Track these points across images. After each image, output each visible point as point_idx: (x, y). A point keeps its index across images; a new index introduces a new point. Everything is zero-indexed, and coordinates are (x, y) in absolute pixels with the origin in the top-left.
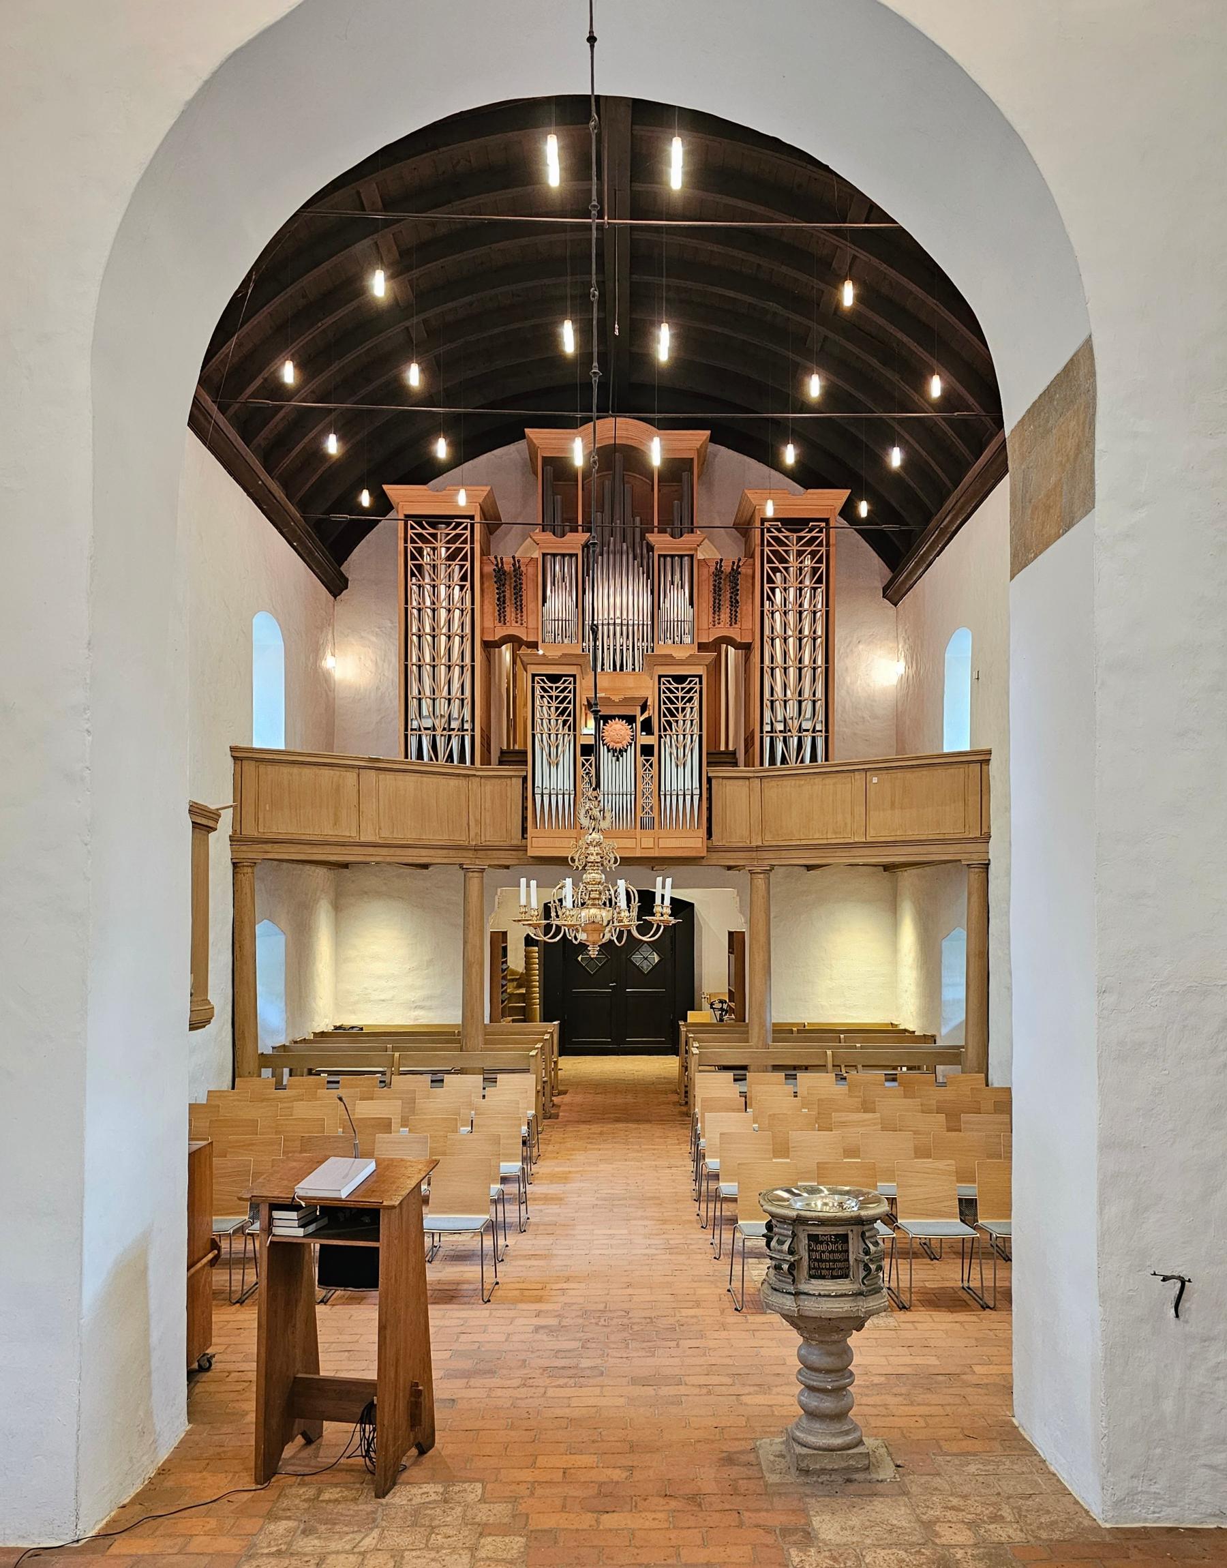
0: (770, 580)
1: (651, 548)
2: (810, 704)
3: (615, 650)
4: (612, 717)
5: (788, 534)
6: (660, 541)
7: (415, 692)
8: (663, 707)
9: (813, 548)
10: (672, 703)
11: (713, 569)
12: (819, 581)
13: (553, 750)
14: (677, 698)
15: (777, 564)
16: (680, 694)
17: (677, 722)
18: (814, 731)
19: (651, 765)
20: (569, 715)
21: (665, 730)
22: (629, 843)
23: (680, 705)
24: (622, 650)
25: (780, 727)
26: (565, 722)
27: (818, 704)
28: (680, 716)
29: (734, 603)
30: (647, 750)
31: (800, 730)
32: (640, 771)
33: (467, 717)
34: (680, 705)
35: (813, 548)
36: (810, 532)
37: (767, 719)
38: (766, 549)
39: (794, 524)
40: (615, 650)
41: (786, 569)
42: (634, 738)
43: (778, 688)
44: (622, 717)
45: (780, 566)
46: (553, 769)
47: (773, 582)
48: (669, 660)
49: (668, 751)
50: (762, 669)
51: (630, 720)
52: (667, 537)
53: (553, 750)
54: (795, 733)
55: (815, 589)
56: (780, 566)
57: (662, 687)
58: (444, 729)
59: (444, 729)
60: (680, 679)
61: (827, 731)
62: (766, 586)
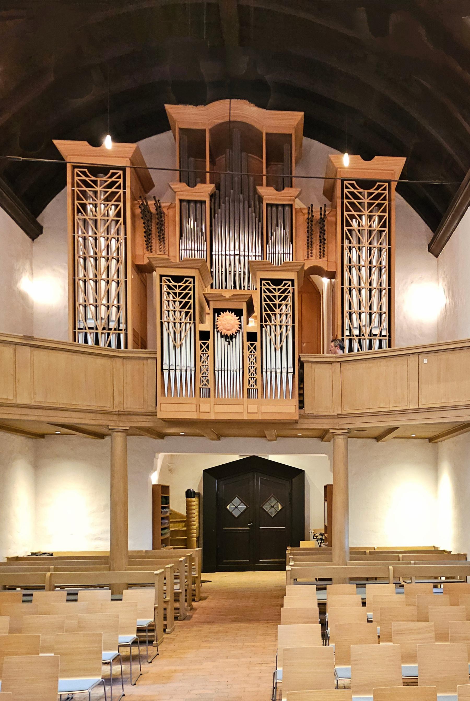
4: (224, 310)
10: (271, 300)
14: (275, 297)
20: (190, 308)
23: (277, 302)
26: (187, 313)
28: (277, 311)
34: (277, 302)
51: (239, 313)
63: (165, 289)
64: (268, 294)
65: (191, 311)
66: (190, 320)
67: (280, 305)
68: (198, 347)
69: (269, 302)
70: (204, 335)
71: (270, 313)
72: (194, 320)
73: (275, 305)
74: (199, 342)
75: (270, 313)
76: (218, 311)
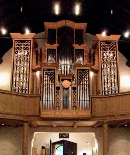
0: (103, 55)
1: (73, 48)
2: (114, 84)
3: (65, 71)
4: (66, 80)
5: (106, 45)
6: (76, 47)
7: (14, 80)
8: (78, 77)
9: (112, 48)
10: (81, 76)
11: (88, 53)
12: (114, 55)
13: (48, 88)
14: (82, 75)
15: (104, 51)
16: (83, 74)
17: (82, 81)
18: (115, 90)
19: (76, 92)
21: (79, 83)
22: (70, 114)
23: (83, 77)
24: (66, 71)
25: (107, 89)
27: (116, 84)
28: (83, 80)
29: (94, 60)
30: (74, 89)
31: (112, 90)
32: (73, 94)
33: (27, 86)
34: (83, 77)
35: (112, 48)
36: (112, 44)
37: (103, 87)
38: (101, 48)
39: (108, 43)
40: (65, 71)
41: (107, 52)
42: (71, 85)
43: (106, 79)
44: (68, 80)
45: (105, 52)
46: (48, 93)
47: (103, 55)
48: (80, 65)
49: (80, 88)
50: (102, 75)
51: (70, 80)
52: (77, 45)
53: (48, 88)
54: (110, 90)
55: (113, 57)
56: (105, 52)
57: (78, 72)
58: (21, 89)
59: (21, 89)
60: (83, 70)
61: (118, 90)
62: (102, 56)
63: (45, 73)
64: (80, 74)
65: (54, 80)
66: (53, 83)
67: (84, 78)
68: (55, 92)
69: (80, 77)
70: (58, 88)
71: (81, 80)
72: (54, 83)
73: (82, 78)
74: (56, 91)
75: (81, 80)
76: (63, 80)
